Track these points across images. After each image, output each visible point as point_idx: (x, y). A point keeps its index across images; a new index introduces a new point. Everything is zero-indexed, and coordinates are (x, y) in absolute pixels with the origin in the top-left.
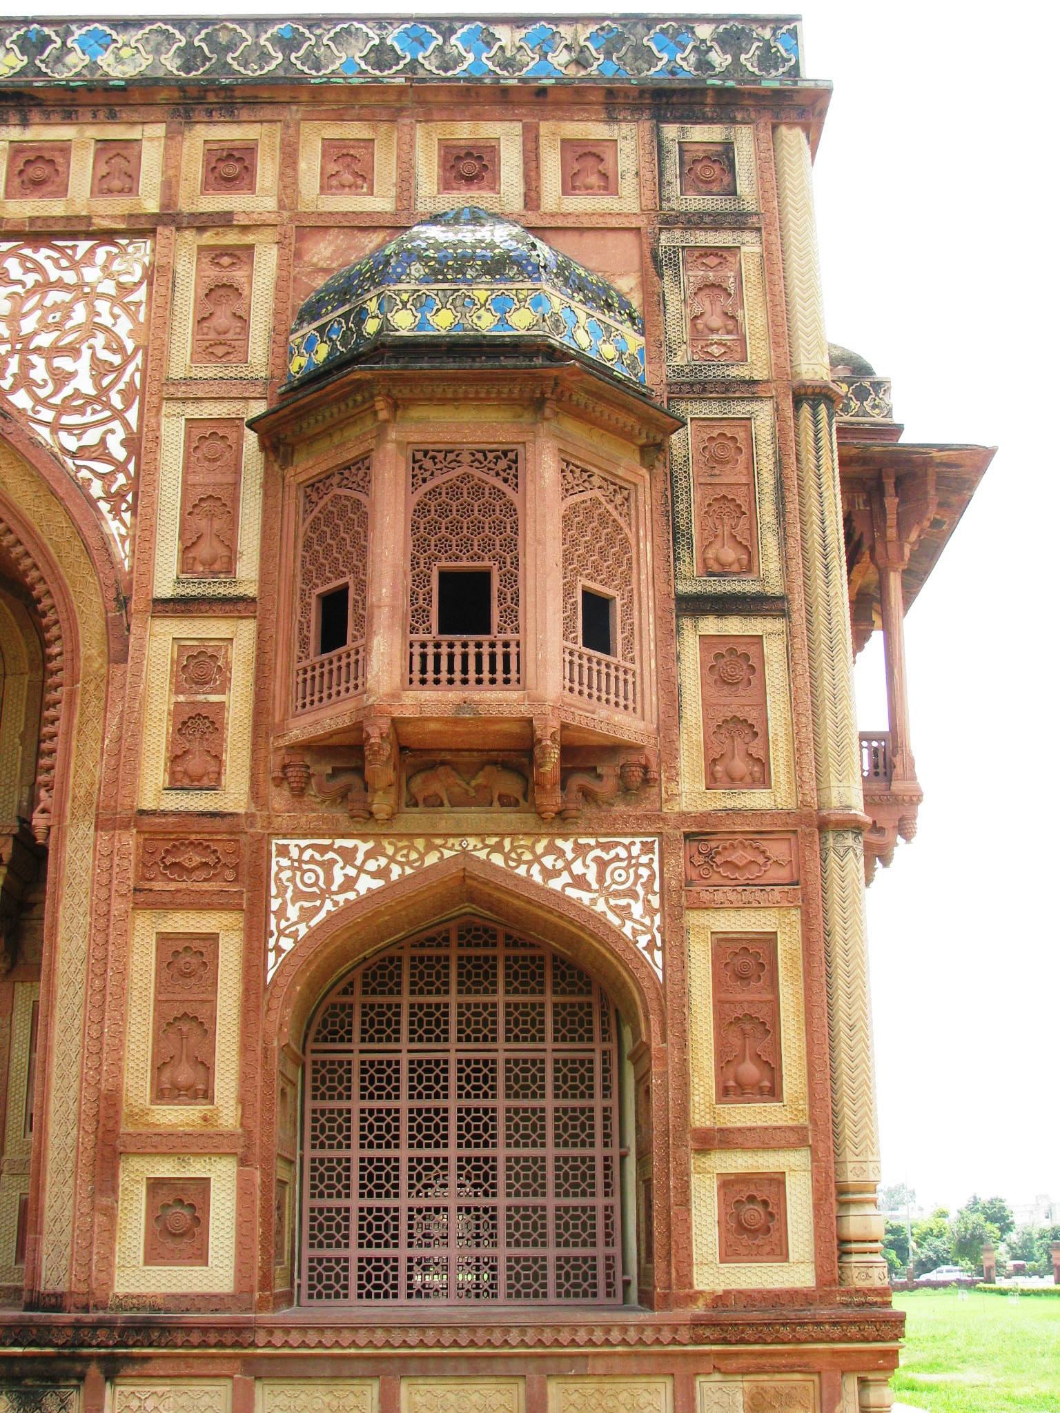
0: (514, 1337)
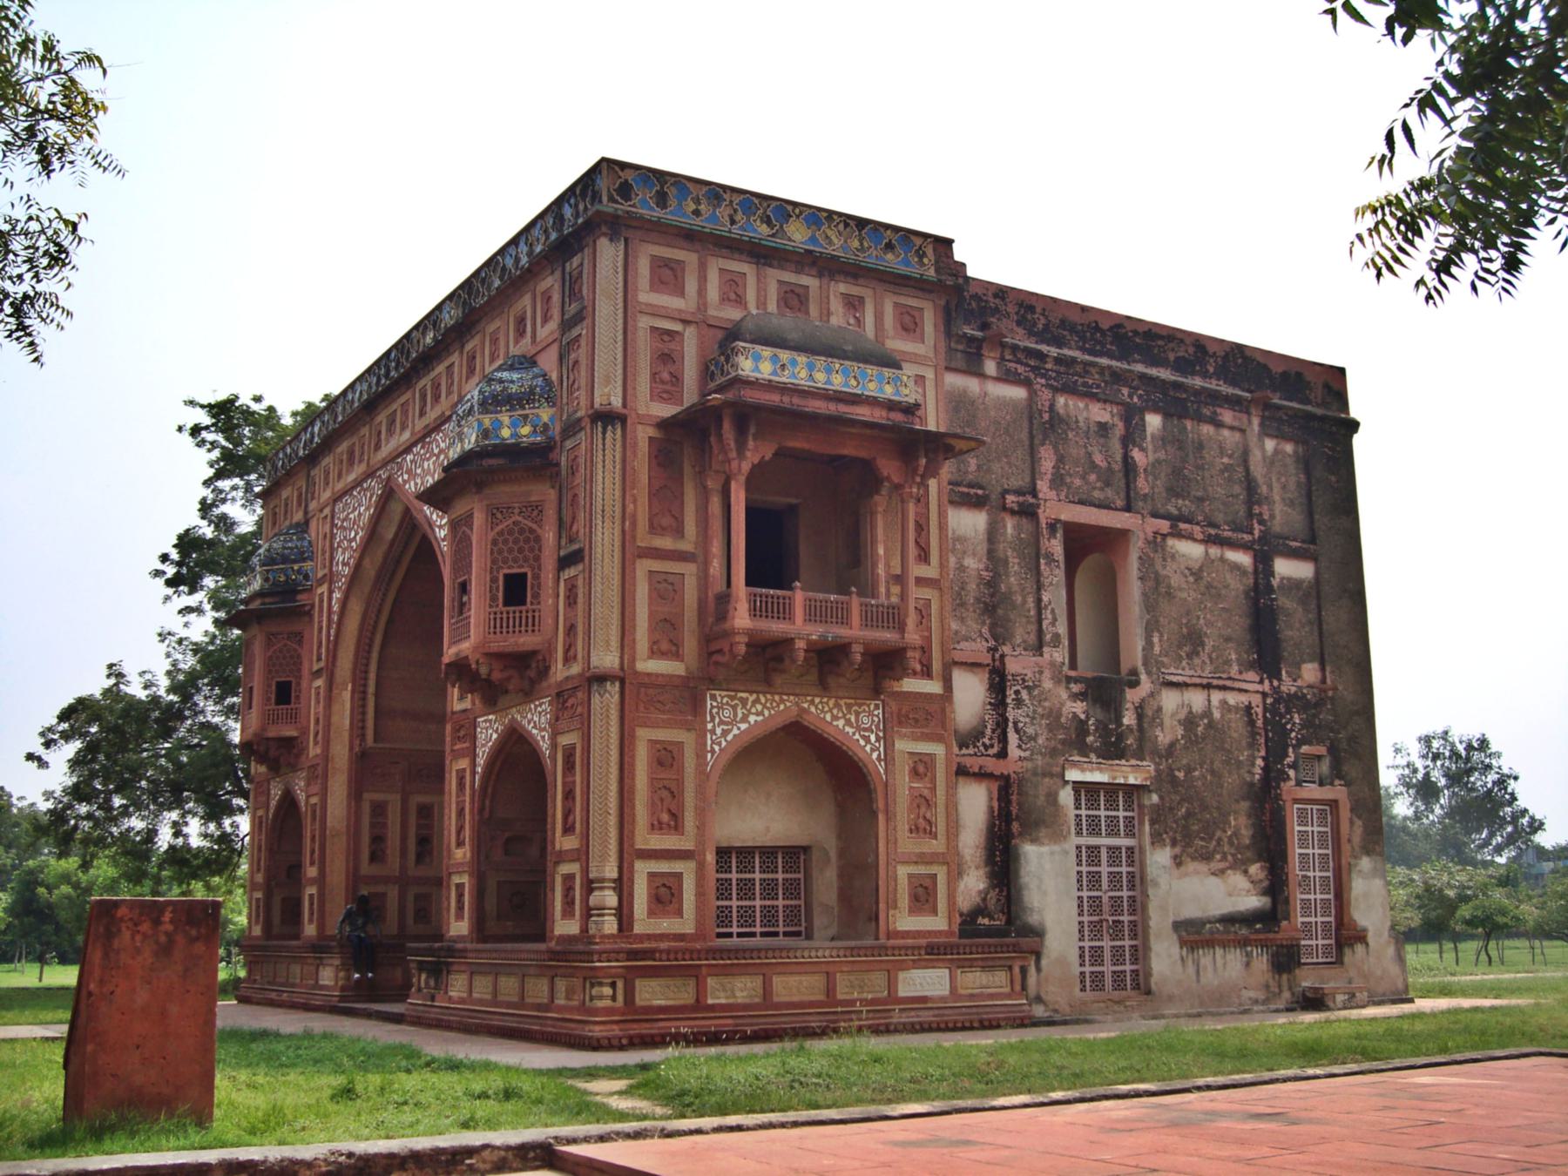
0: (806, 954)
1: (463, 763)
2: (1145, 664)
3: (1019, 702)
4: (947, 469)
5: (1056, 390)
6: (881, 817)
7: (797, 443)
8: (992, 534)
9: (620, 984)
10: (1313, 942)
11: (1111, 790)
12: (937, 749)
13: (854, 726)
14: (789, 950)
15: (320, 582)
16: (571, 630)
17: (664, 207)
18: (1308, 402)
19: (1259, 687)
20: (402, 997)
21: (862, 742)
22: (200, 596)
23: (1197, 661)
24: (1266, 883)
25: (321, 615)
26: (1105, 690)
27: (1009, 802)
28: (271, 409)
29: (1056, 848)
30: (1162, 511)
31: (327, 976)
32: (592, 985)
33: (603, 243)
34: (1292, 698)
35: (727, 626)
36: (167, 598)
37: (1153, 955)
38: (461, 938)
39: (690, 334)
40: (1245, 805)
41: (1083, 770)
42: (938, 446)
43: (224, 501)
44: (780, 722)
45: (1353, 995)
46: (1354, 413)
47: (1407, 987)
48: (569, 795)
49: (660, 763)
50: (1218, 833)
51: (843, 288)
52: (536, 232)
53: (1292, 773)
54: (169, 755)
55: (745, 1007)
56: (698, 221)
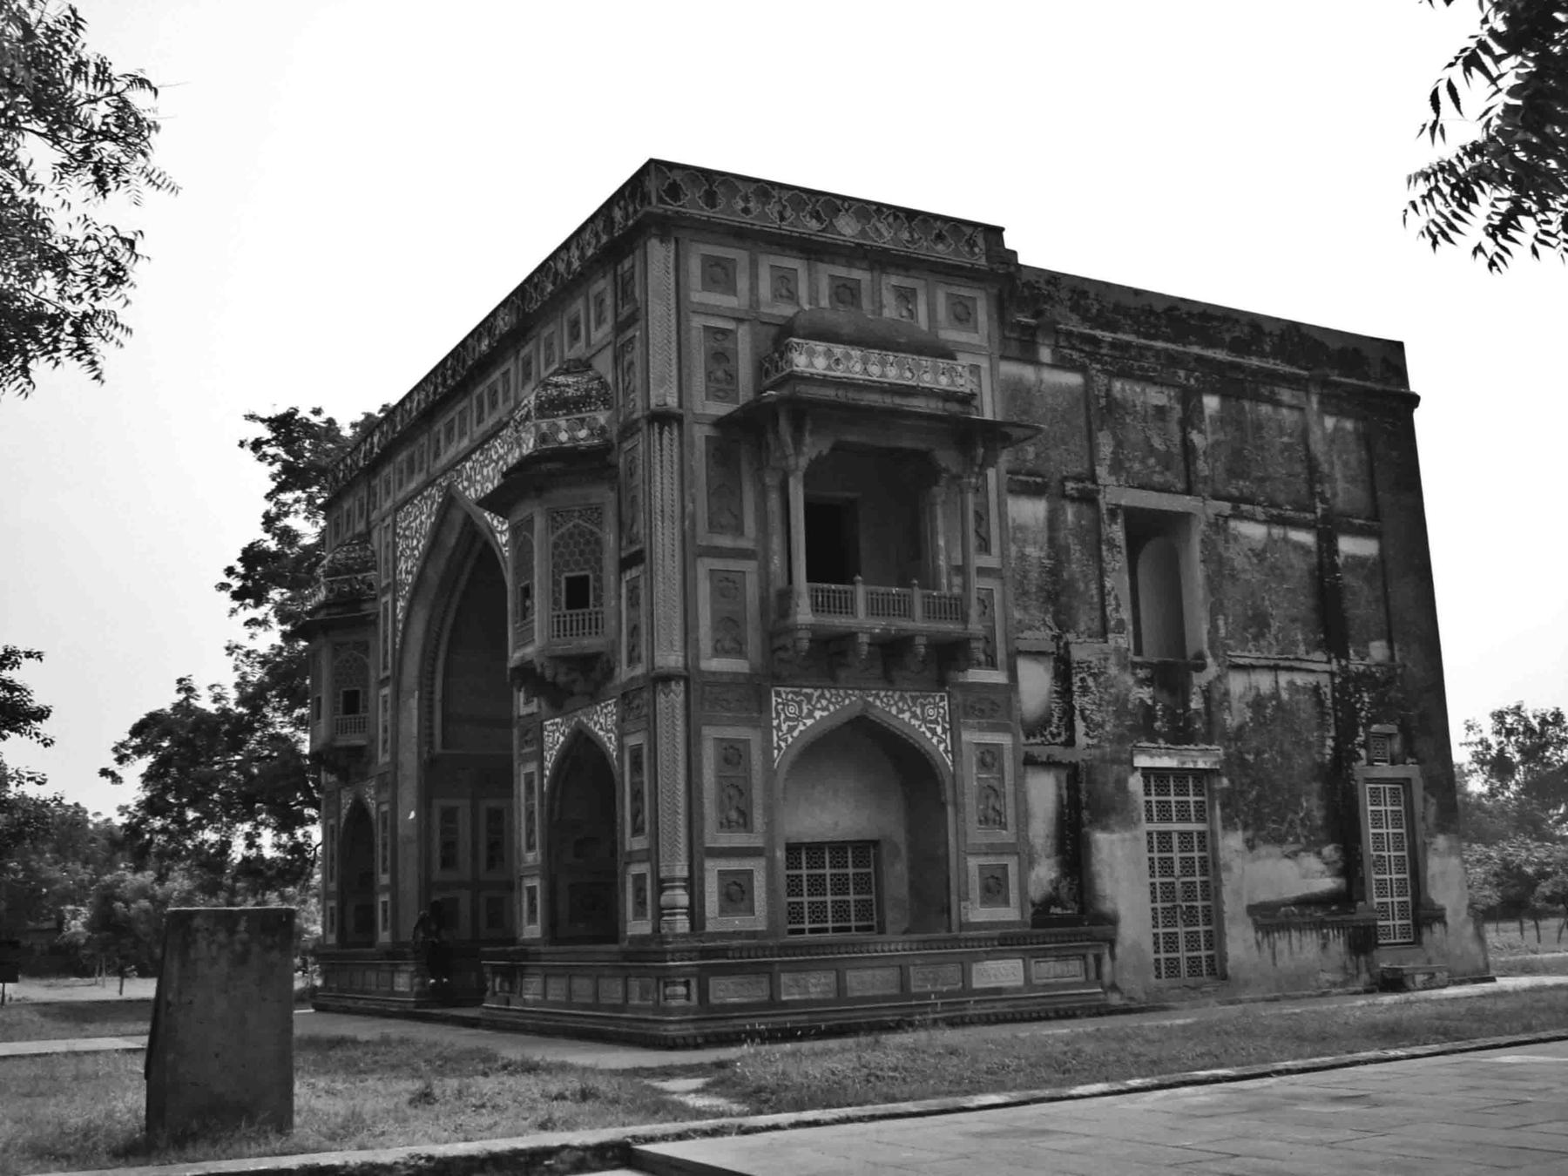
1: (532, 767)
2: (1211, 647)
3: (1085, 690)
4: (1005, 458)
5: (1113, 375)
6: (950, 809)
7: (851, 438)
8: (1053, 521)
9: (693, 983)
10: (1390, 923)
11: (1181, 775)
12: (1005, 740)
13: (922, 719)
14: (862, 944)
15: (384, 591)
16: (634, 631)
17: (713, 206)
18: (1367, 378)
19: (1327, 667)
20: (477, 1002)
21: (929, 735)
22: (265, 610)
23: (1263, 643)
24: (1340, 865)
25: (386, 624)
26: (1171, 675)
27: (1078, 790)
28: (331, 421)
29: (1127, 835)
30: (1223, 493)
31: (403, 982)
32: (666, 985)
33: (654, 246)
34: (1360, 676)
35: (790, 621)
36: (233, 611)
37: (1228, 940)
38: (533, 942)
39: (743, 332)
40: (1316, 786)
41: (1152, 756)
42: (995, 435)
43: (286, 514)
44: (844, 717)
45: (1432, 975)
46: (1414, 387)
47: (1487, 966)
48: (637, 795)
49: (727, 760)
50: (1290, 816)
51: (895, 280)
52: (587, 235)
53: (1363, 752)
54: (241, 766)
55: (818, 1002)
56: (748, 219)
